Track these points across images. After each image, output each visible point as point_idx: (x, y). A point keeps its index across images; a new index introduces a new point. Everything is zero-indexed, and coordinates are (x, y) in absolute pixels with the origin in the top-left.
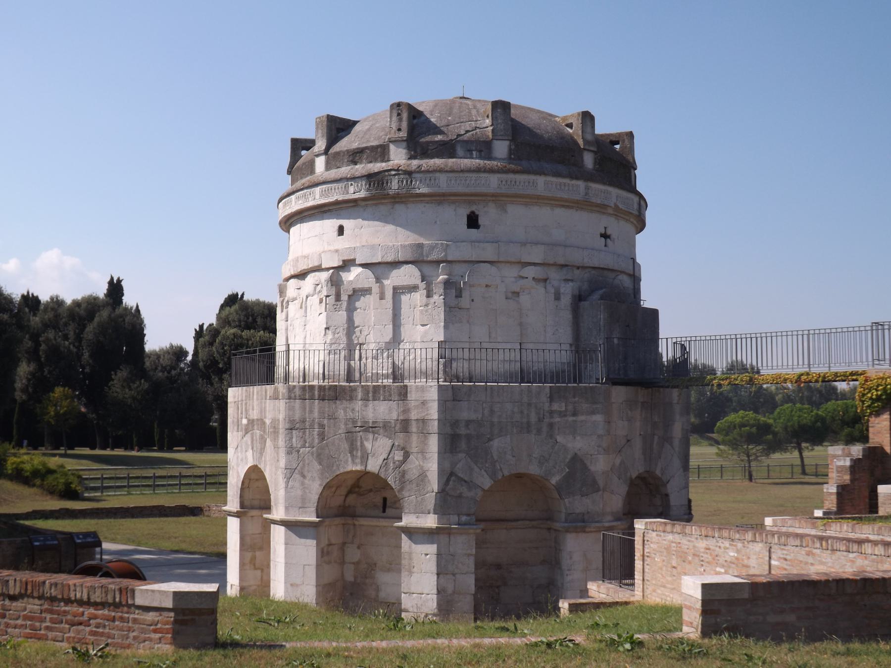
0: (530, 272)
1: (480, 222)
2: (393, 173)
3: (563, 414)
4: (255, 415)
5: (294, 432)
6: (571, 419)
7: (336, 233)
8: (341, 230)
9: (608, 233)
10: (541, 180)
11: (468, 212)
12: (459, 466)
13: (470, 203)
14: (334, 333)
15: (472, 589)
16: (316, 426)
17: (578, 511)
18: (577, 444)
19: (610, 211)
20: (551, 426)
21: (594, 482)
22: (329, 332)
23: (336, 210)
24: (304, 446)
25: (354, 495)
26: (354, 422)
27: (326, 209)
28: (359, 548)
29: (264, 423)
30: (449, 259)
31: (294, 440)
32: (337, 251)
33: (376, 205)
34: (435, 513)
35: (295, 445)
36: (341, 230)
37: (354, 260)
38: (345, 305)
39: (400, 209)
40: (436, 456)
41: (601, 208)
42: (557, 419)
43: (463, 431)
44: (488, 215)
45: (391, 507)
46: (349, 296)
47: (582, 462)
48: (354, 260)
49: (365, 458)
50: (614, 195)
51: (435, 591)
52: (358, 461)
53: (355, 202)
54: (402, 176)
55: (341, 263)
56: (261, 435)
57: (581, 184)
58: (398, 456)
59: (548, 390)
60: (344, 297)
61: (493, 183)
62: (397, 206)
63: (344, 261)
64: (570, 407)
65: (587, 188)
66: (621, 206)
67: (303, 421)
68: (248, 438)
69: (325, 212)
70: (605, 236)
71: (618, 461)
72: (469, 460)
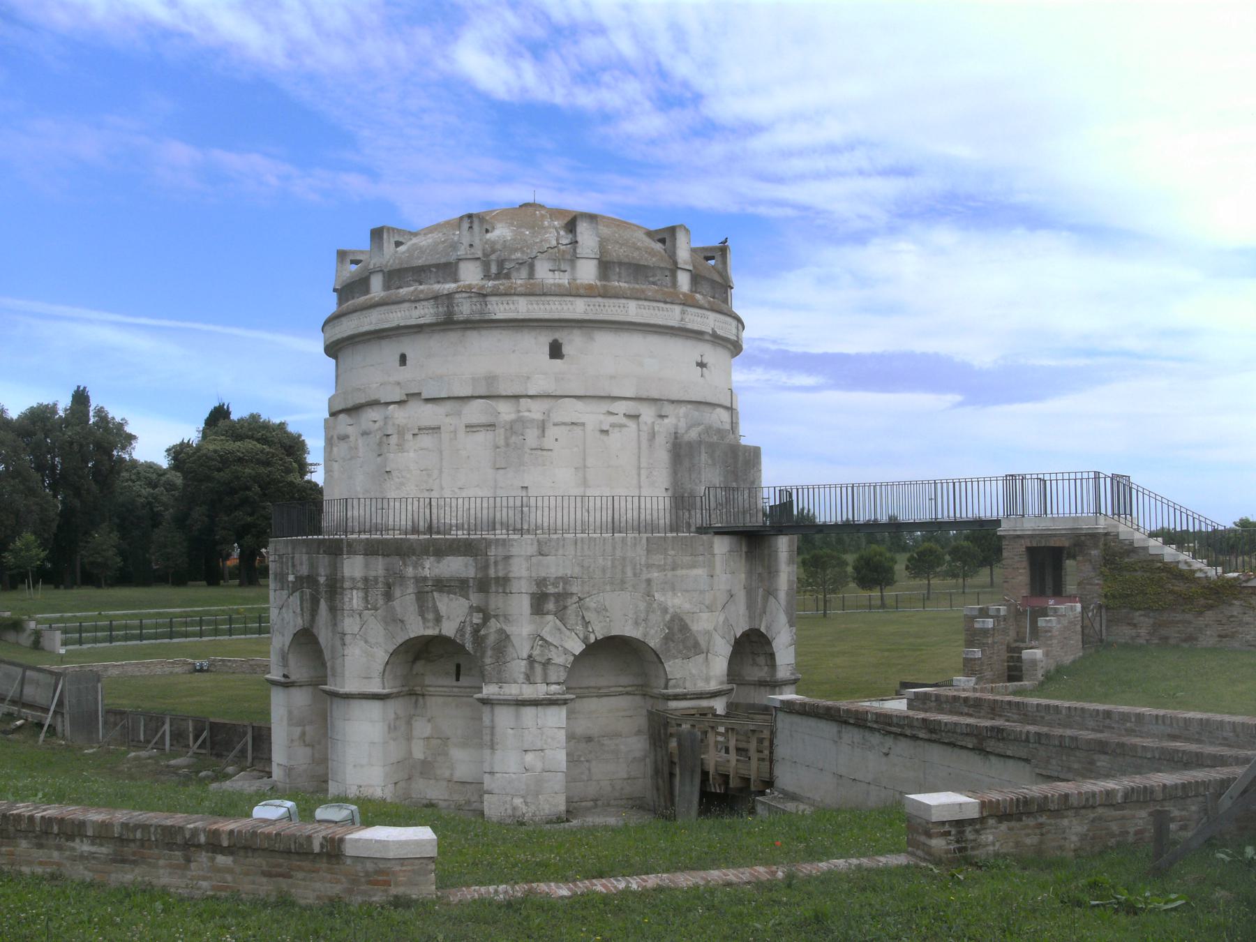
0: (621, 407)
1: (565, 350)
2: (464, 295)
3: (662, 568)
4: (304, 570)
5: (355, 592)
6: (670, 574)
8: (403, 359)
9: (705, 361)
10: (632, 305)
11: (550, 340)
12: (547, 629)
15: (564, 766)
16: (380, 585)
17: (678, 676)
18: (677, 602)
19: (707, 337)
20: (649, 581)
21: (696, 645)
24: (367, 609)
25: (422, 662)
26: (425, 579)
28: (429, 721)
29: (316, 582)
30: (530, 393)
31: (355, 601)
32: (399, 384)
33: (444, 330)
35: (355, 606)
36: (403, 359)
37: (419, 394)
41: (697, 335)
42: (655, 574)
43: (551, 590)
44: (573, 343)
47: (681, 620)
48: (419, 394)
49: (438, 619)
50: (709, 322)
52: (431, 624)
53: (419, 329)
55: (404, 398)
56: (311, 594)
57: (677, 309)
58: (477, 619)
59: (644, 541)
60: (409, 436)
61: (578, 308)
62: (469, 333)
64: (670, 560)
65: (683, 312)
66: (719, 332)
67: (366, 580)
68: (295, 600)
70: (701, 365)
71: (721, 619)
72: (558, 622)
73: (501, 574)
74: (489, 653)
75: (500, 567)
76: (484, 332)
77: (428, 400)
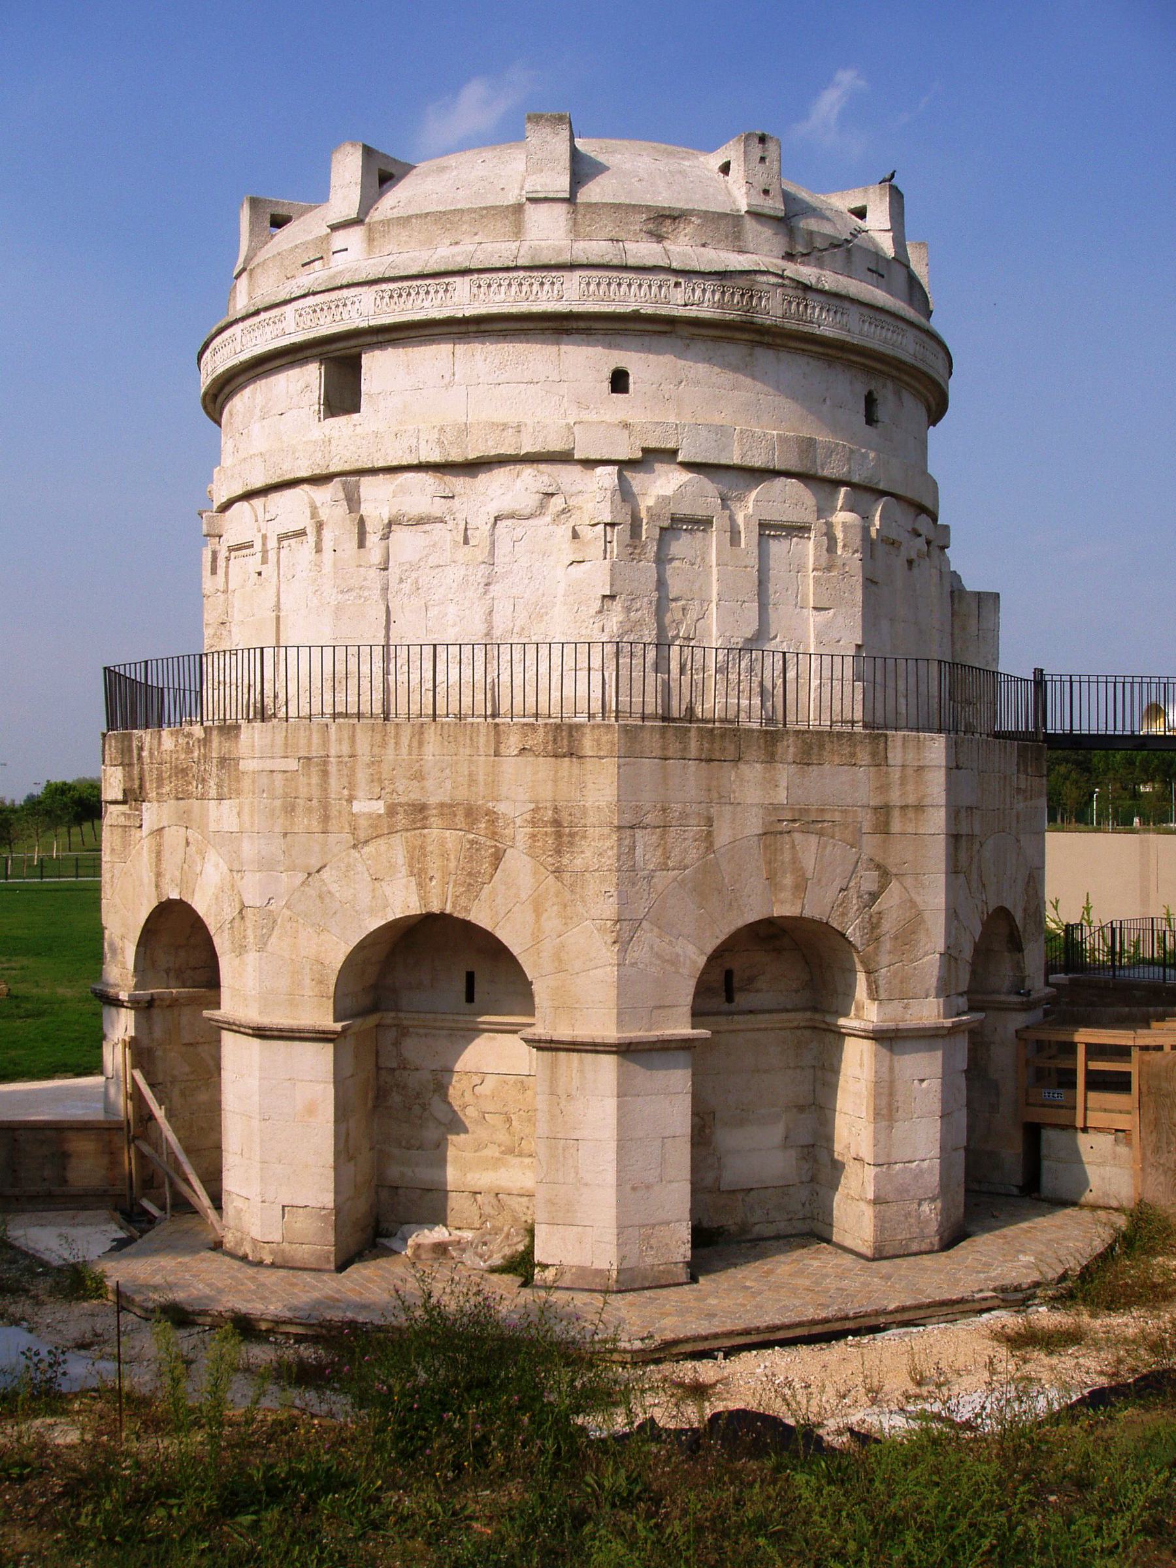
2: (773, 280)
5: (639, 833)
7: (607, 386)
8: (619, 381)
13: (869, 371)
14: (628, 610)
22: (617, 606)
23: (607, 333)
27: (582, 325)
31: (639, 851)
32: (626, 426)
33: (715, 339)
34: (937, 996)
36: (619, 381)
37: (675, 452)
38: (652, 549)
39: (765, 357)
40: (941, 879)
45: (742, 989)
46: (662, 529)
48: (675, 452)
51: (936, 1152)
54: (791, 292)
55: (639, 455)
58: (868, 881)
62: (759, 351)
63: (645, 450)
69: (568, 332)
73: (911, 800)
74: (887, 945)
75: (910, 788)
76: (783, 355)
77: (689, 466)
